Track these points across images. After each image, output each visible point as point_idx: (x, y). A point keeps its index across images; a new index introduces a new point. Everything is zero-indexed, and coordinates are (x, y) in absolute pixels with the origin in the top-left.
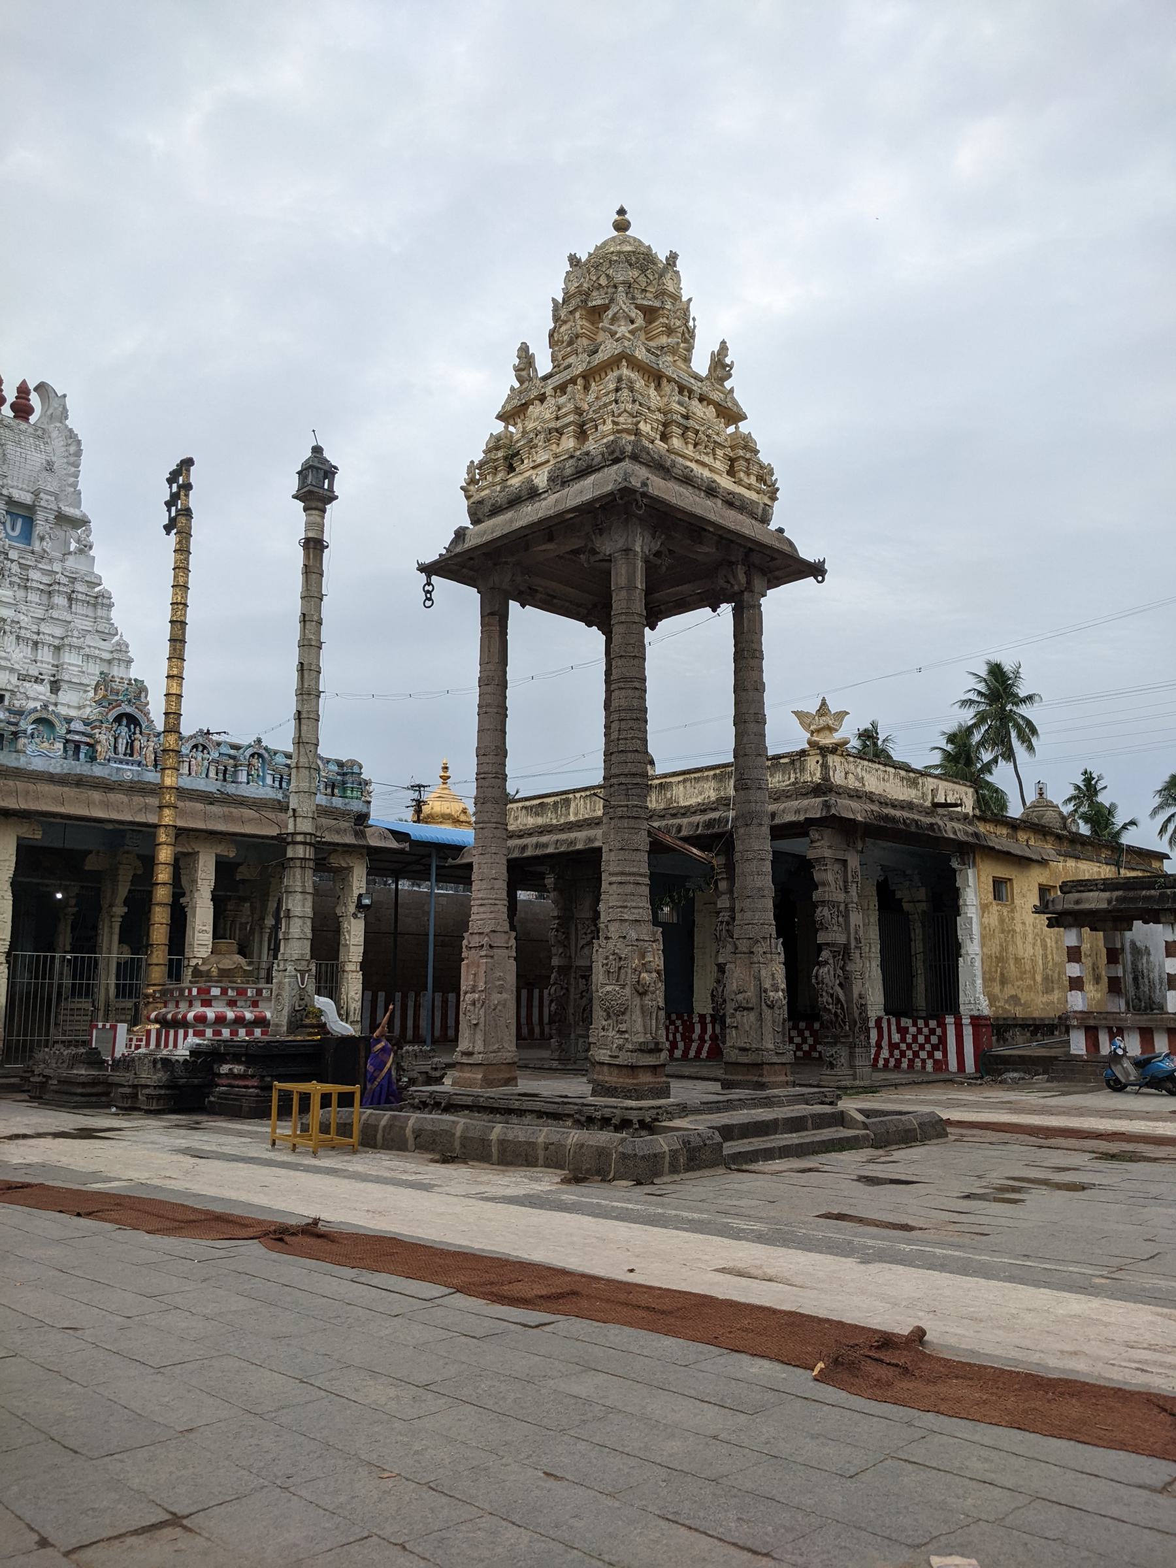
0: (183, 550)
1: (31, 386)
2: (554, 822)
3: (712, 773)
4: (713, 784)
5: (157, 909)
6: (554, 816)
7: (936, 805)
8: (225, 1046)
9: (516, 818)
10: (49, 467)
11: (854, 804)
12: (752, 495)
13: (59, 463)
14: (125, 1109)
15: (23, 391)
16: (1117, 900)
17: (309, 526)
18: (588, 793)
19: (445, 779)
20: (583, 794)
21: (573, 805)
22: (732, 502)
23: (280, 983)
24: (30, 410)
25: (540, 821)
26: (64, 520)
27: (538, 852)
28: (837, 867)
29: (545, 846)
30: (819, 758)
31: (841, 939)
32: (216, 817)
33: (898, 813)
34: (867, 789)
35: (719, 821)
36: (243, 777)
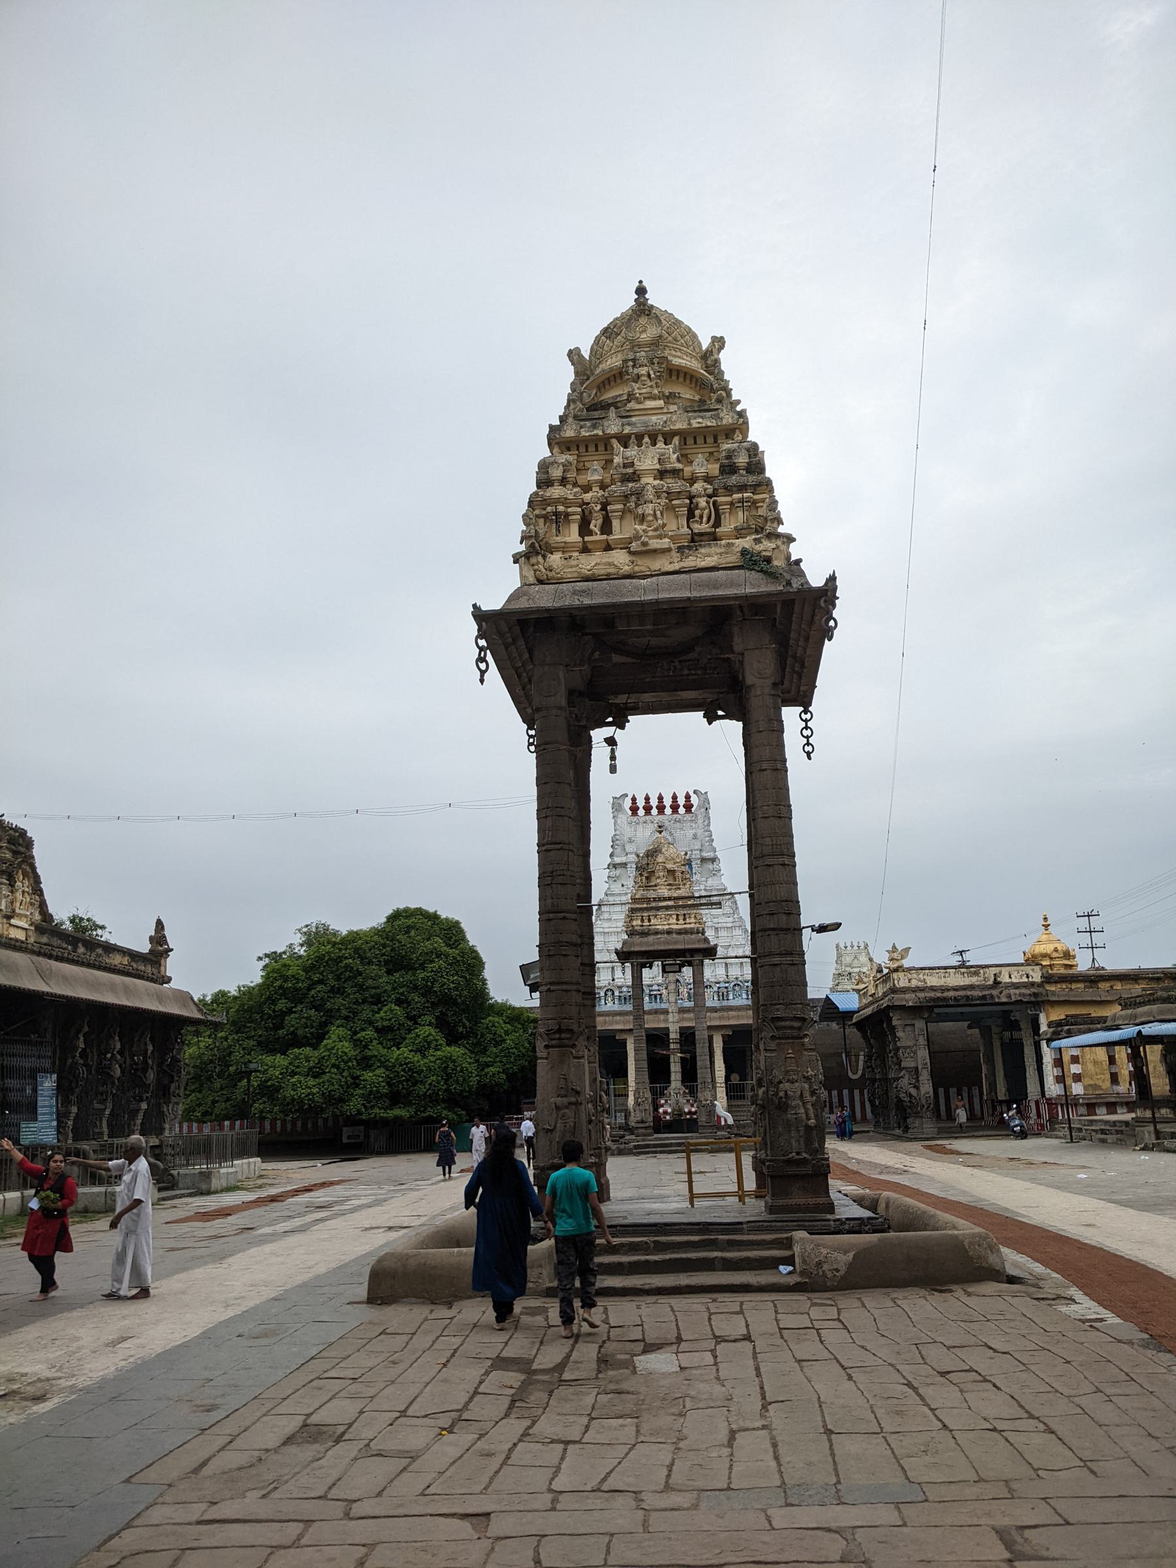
1: (691, 794)
5: (672, 1065)
7: (996, 983)
10: (695, 837)
11: (907, 996)
12: (692, 926)
13: (700, 832)
15: (688, 797)
19: (1046, 926)
22: (679, 932)
24: (692, 806)
26: (704, 860)
28: (909, 1028)
31: (913, 1065)
32: (715, 1018)
33: (951, 994)
34: (929, 984)
36: (731, 997)
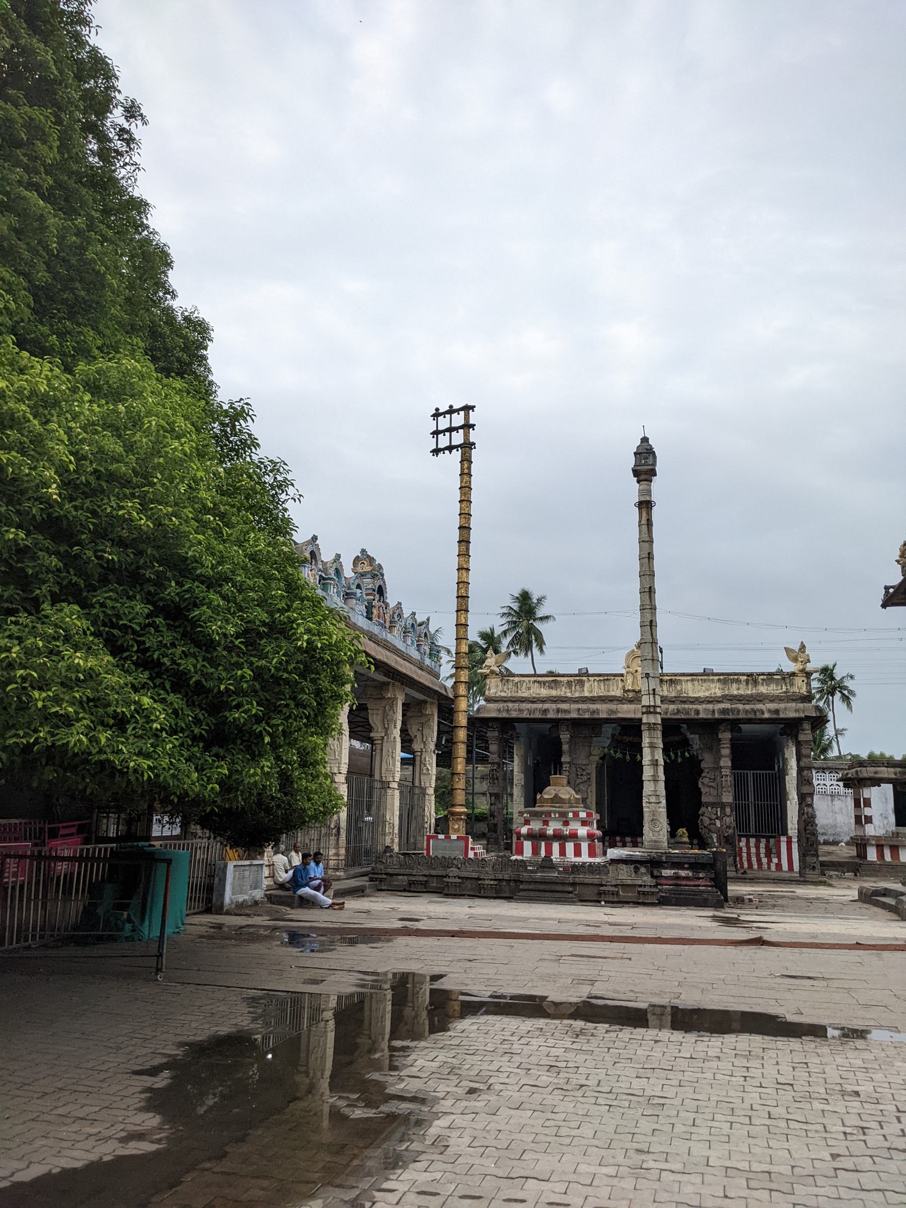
0: (466, 474)
2: (569, 695)
3: (716, 678)
4: (718, 685)
6: (568, 691)
8: (666, 857)
9: (529, 689)
14: (613, 902)
16: (900, 772)
17: (641, 492)
18: (602, 678)
20: (597, 678)
21: (587, 685)
23: (653, 813)
25: (554, 693)
27: (560, 716)
29: (566, 711)
30: (804, 679)
35: (732, 710)
